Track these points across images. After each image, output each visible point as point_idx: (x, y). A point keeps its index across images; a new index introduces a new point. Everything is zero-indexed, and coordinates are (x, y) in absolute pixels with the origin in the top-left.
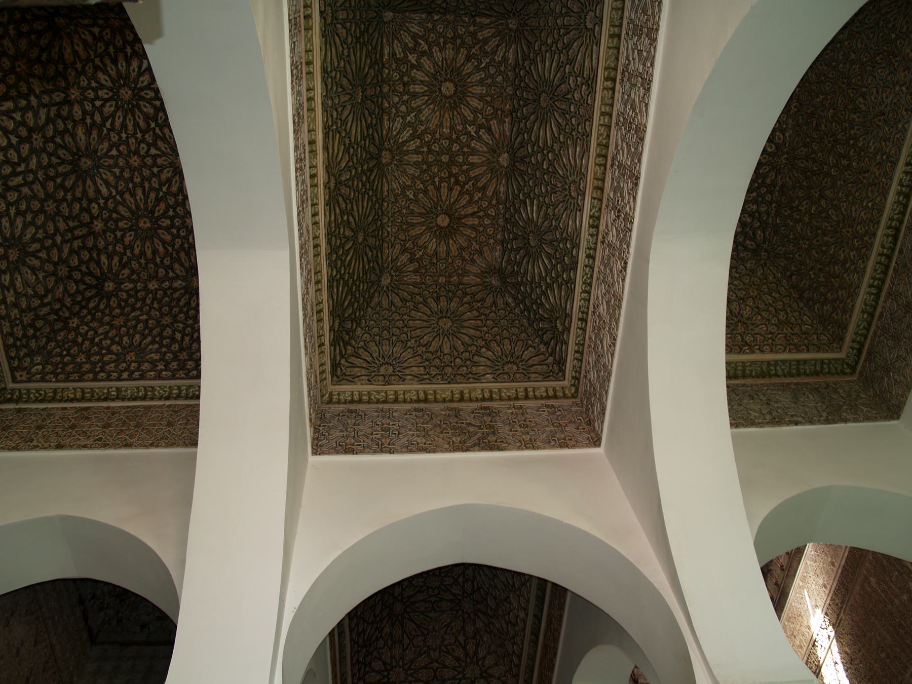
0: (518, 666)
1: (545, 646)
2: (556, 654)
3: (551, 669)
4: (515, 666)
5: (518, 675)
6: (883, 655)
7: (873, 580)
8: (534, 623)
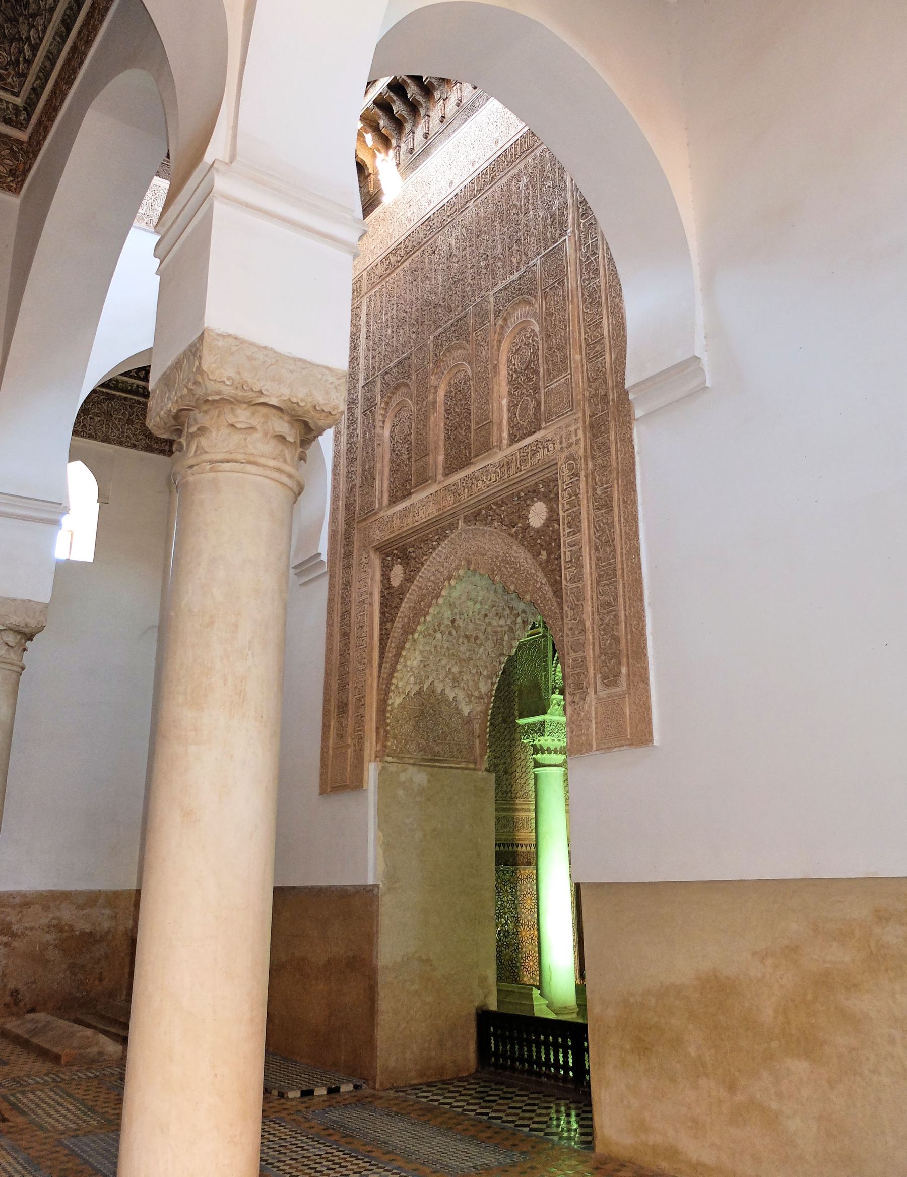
0: (29, 62)
1: (74, 48)
2: (82, 62)
3: (70, 83)
4: (25, 61)
5: (24, 75)
6: (483, 264)
7: (524, 180)
8: (70, 8)
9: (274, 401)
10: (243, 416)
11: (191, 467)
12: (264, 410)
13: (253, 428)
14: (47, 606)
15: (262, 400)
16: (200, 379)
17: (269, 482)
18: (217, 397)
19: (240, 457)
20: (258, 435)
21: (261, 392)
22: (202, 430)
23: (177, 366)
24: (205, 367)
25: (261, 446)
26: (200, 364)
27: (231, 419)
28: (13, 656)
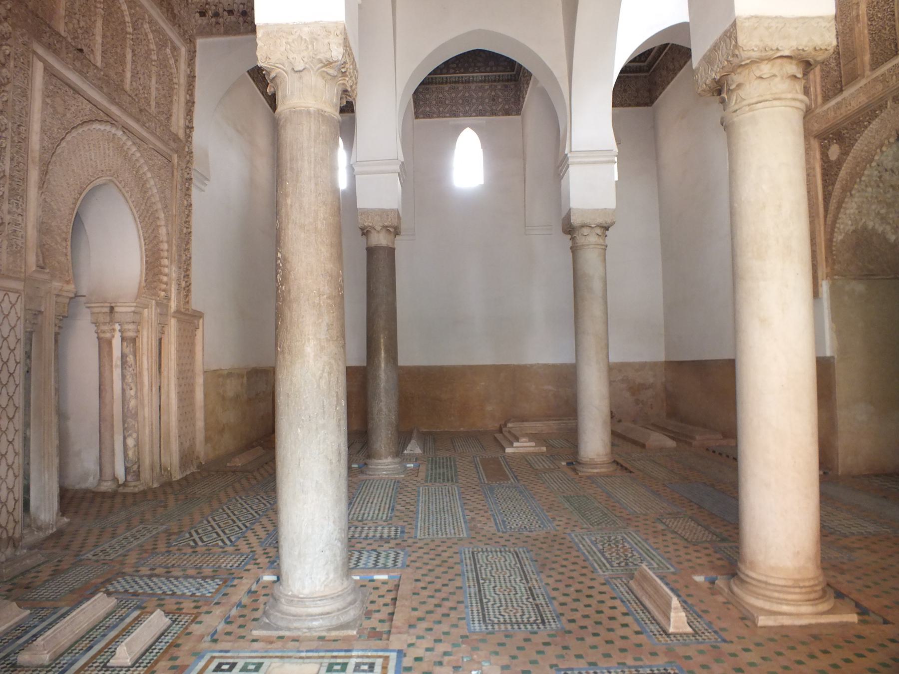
9: (787, 53)
10: (765, 69)
11: (735, 111)
12: (779, 61)
13: (775, 76)
14: (614, 210)
15: (779, 54)
16: (737, 52)
17: (788, 109)
18: (748, 61)
19: (768, 97)
20: (777, 80)
21: (777, 49)
22: (739, 86)
23: (715, 48)
24: (740, 43)
25: (781, 86)
26: (736, 42)
27: (758, 74)
28: (601, 241)
